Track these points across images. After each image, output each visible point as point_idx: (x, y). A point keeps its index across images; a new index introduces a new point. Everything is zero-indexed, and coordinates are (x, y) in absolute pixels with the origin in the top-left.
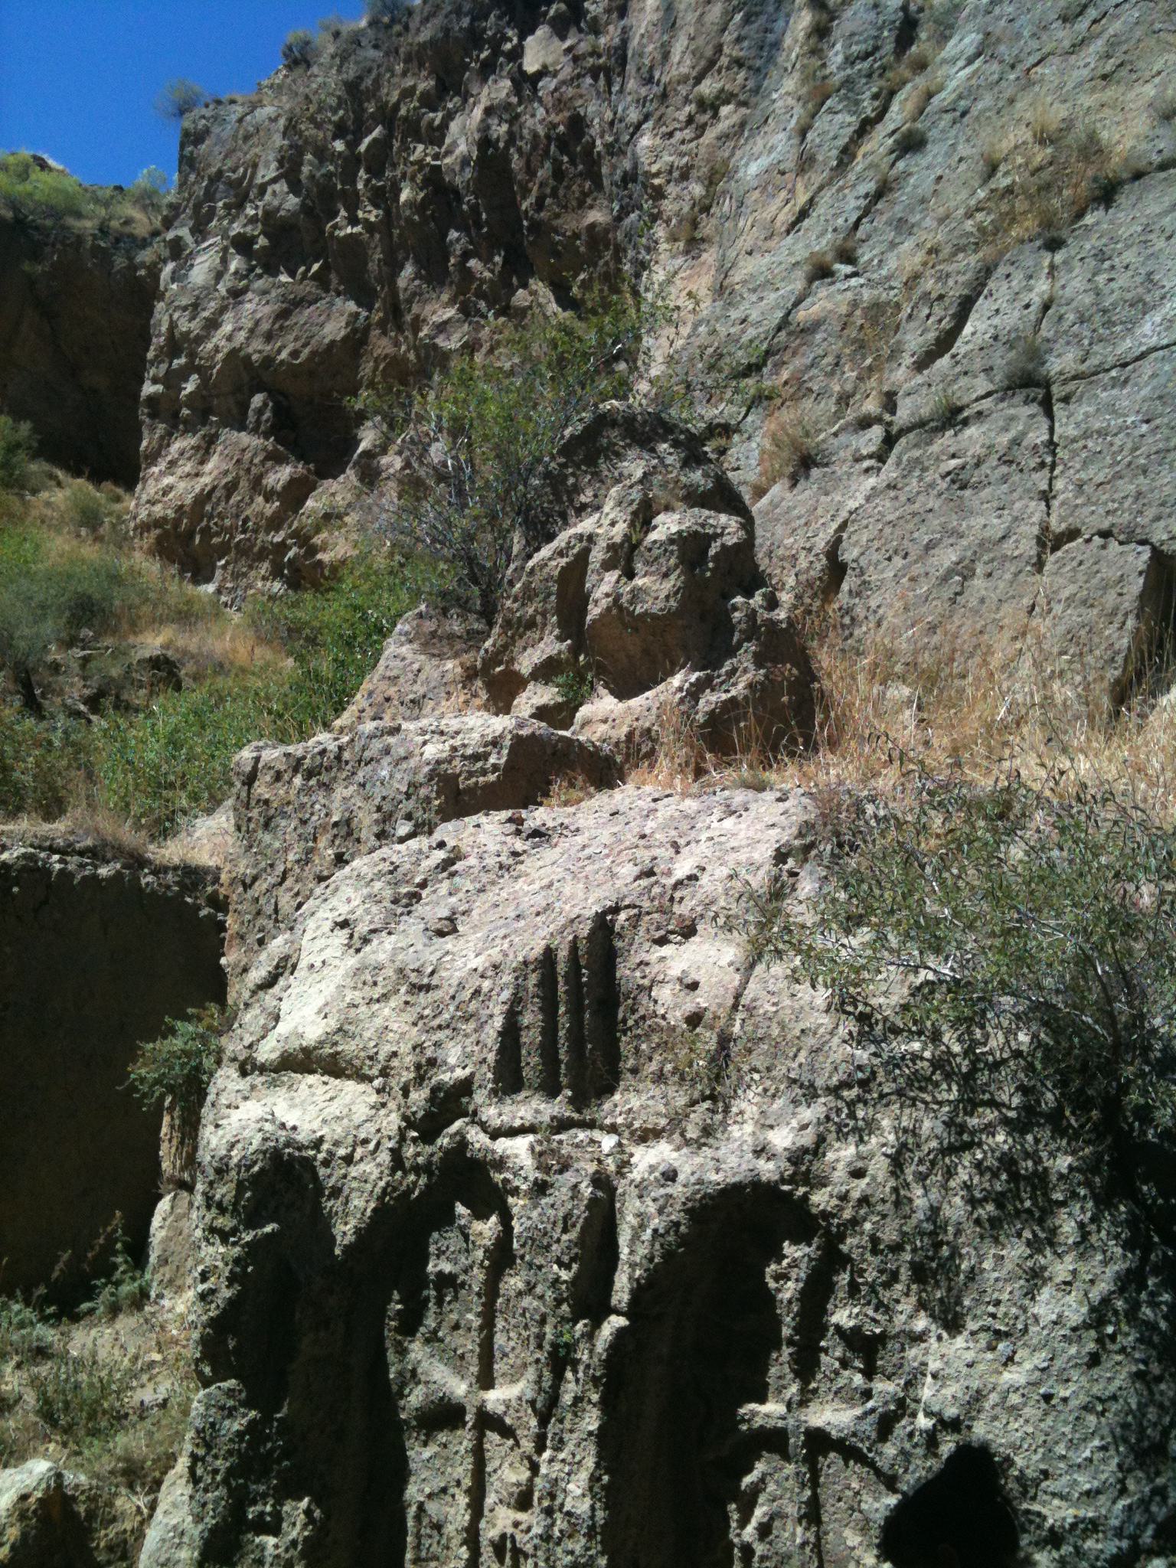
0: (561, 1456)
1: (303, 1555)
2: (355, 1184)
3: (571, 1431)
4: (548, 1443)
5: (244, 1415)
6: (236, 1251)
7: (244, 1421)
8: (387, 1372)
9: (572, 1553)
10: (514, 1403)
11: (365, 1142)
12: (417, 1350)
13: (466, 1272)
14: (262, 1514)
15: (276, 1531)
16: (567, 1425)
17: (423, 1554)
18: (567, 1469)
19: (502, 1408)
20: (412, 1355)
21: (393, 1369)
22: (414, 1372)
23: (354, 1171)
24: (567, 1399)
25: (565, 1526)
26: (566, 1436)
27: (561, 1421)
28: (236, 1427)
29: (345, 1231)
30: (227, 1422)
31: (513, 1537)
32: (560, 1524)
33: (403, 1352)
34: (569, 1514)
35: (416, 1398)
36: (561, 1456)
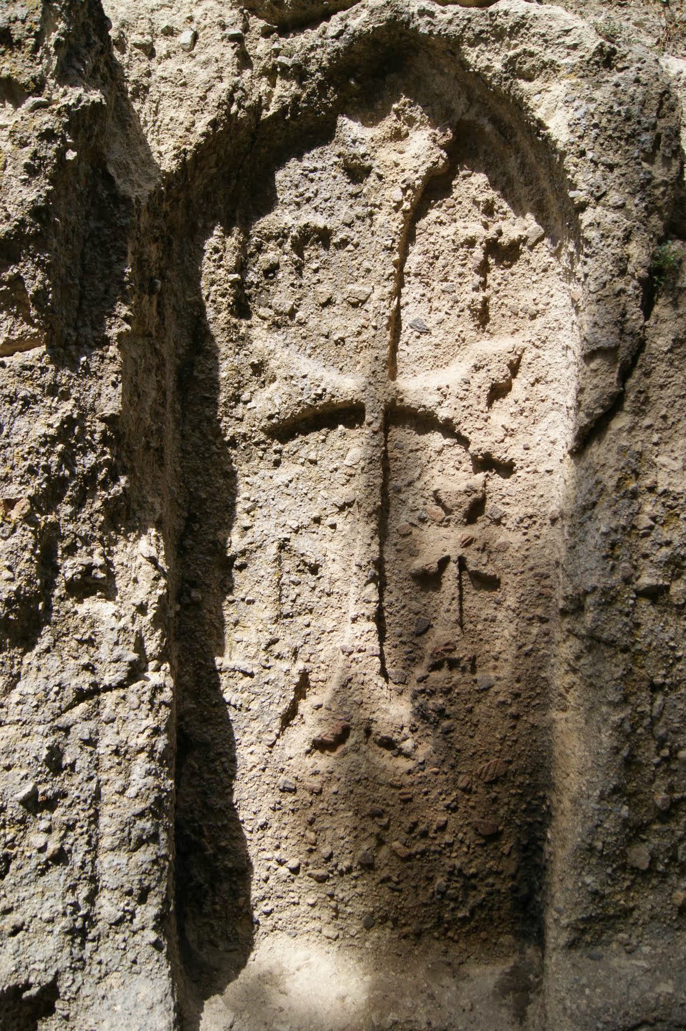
0: (647, 422)
1: (156, 622)
2: (166, 88)
3: (662, 387)
4: (627, 406)
5: (53, 411)
6: (45, 121)
7: (55, 420)
8: (216, 368)
9: (668, 544)
10: (455, 389)
11: (169, 32)
12: (263, 340)
13: (349, 225)
14: (89, 568)
15: (108, 591)
16: (657, 378)
17: (287, 609)
18: (655, 438)
19: (437, 398)
20: (257, 345)
21: (224, 365)
22: (258, 368)
23: (159, 70)
24: (661, 342)
25: (659, 510)
26: (654, 394)
27: (647, 374)
28: (39, 429)
29: (165, 152)
30: (21, 423)
31: (462, 562)
32: (650, 507)
33: (242, 341)
34: (665, 493)
35: (267, 402)
36: (647, 422)
